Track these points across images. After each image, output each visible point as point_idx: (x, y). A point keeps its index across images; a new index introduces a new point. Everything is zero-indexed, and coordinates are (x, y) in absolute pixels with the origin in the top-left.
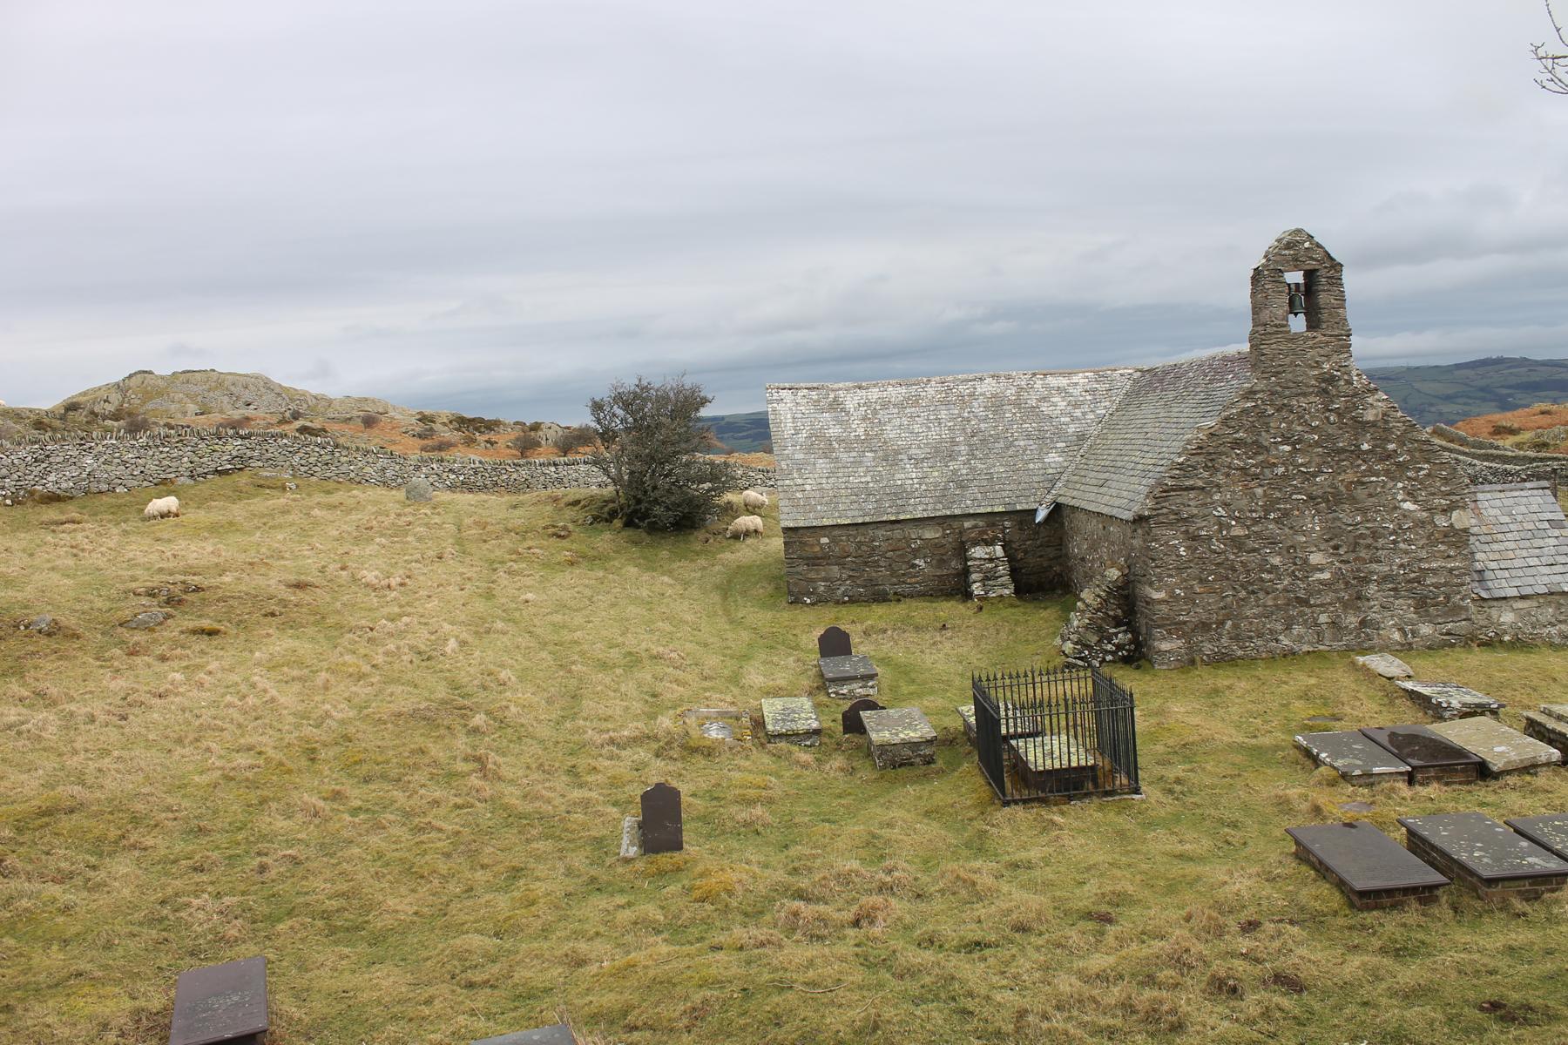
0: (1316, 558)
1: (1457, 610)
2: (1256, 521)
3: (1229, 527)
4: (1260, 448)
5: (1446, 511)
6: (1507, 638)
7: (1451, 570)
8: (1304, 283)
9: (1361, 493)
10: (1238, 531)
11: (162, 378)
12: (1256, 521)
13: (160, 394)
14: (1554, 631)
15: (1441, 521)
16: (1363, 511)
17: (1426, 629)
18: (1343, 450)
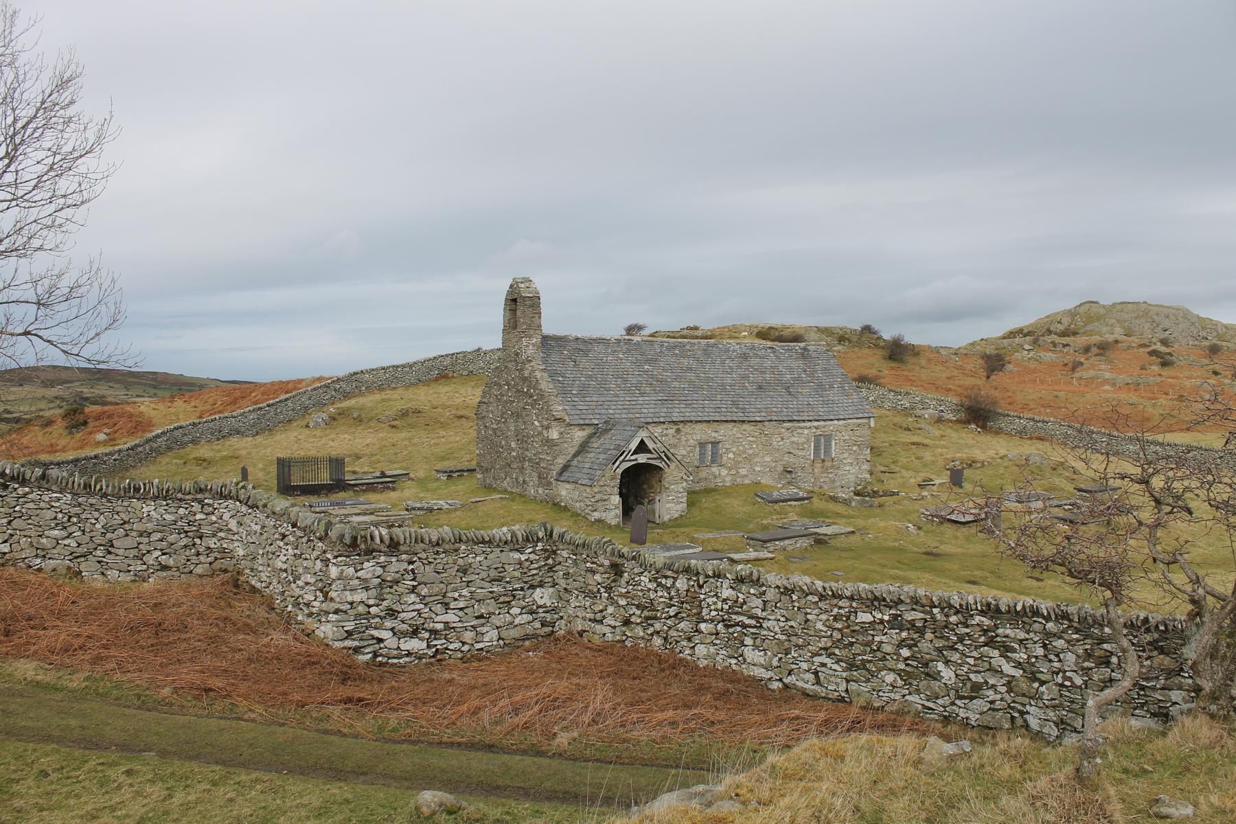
0: (513, 445)
2: (499, 422)
4: (501, 387)
8: (520, 305)
9: (524, 413)
11: (1104, 307)
12: (499, 422)
13: (1098, 319)
14: (578, 505)
15: (545, 432)
17: (540, 491)
18: (519, 391)
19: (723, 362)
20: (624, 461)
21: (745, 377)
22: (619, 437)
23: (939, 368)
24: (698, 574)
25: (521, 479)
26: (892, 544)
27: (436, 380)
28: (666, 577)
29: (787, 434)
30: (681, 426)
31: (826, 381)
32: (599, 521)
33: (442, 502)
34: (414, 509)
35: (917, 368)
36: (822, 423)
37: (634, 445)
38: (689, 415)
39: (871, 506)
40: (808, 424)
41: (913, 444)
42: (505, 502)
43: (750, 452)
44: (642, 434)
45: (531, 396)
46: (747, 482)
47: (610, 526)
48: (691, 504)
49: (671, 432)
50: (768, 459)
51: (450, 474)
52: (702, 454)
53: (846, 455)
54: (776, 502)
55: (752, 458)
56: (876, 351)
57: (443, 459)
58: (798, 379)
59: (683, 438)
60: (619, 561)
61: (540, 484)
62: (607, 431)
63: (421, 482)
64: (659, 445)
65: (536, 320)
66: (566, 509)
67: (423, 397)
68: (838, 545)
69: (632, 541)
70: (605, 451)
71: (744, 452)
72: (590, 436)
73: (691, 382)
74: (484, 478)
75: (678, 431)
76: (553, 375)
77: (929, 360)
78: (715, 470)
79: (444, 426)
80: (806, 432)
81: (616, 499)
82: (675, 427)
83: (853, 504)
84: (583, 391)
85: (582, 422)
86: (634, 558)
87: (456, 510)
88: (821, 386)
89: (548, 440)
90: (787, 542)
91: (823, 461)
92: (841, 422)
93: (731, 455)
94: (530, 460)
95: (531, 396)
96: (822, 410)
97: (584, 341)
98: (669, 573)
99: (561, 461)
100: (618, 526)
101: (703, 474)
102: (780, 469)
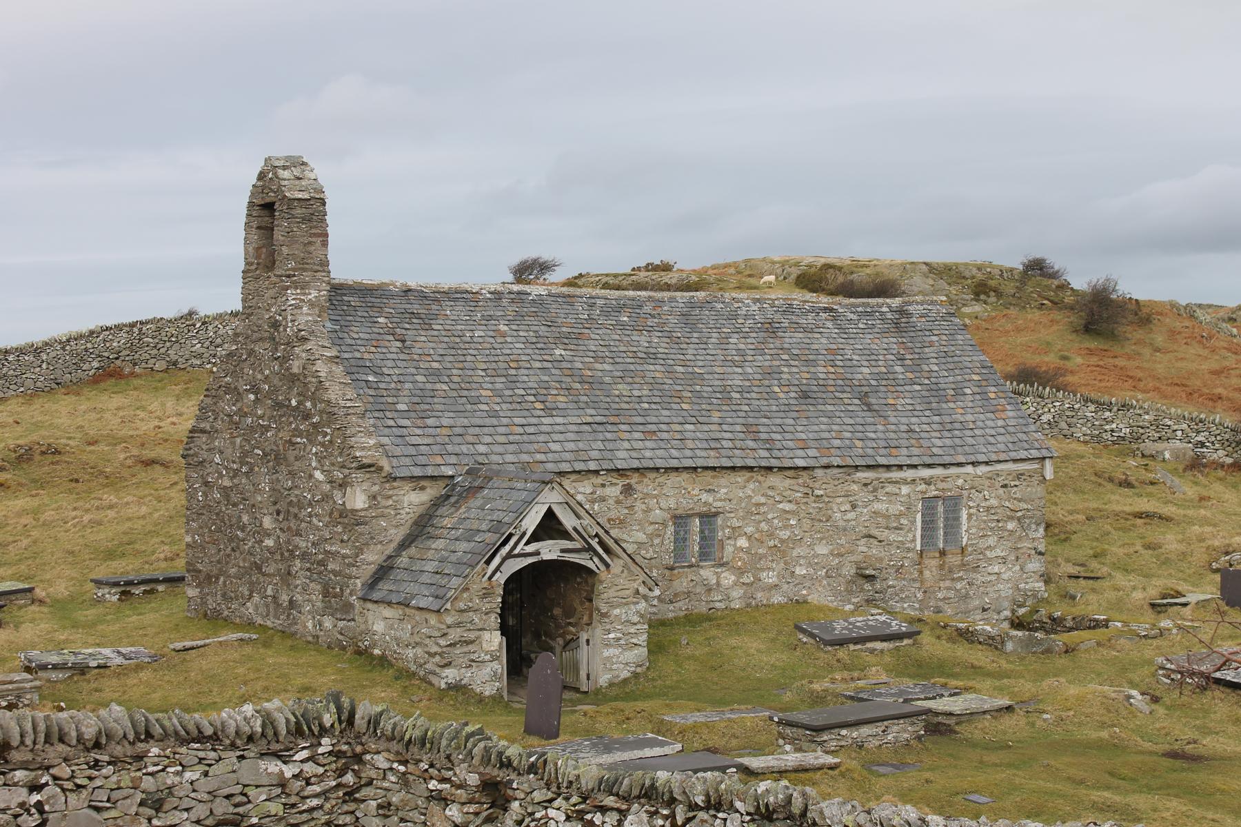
0: (268, 522)
1: (348, 607)
2: (236, 473)
3: (221, 476)
4: (239, 396)
5: (343, 485)
6: (377, 652)
7: (344, 557)
8: (282, 216)
10: (227, 483)
12: (236, 473)
14: (410, 653)
15: (337, 495)
16: (292, 474)
17: (328, 623)
18: (278, 405)
19: (724, 342)
20: (510, 555)
21: (770, 373)
22: (499, 504)
23: (1195, 349)
24: (672, 802)
25: (284, 598)
26: (1094, 735)
27: (96, 380)
28: (603, 810)
29: (863, 496)
30: (634, 480)
31: (948, 382)
32: (457, 688)
33: (107, 651)
34: (44, 667)
35: (1147, 352)
36: (939, 471)
37: (531, 522)
38: (651, 454)
39: (1048, 651)
40: (909, 474)
41: (1139, 515)
42: (248, 650)
43: (784, 534)
44: (551, 497)
45: (307, 416)
46: (777, 599)
47: (481, 699)
48: (656, 648)
49: (613, 491)
50: (822, 549)
51: (125, 589)
52: (681, 541)
53: (991, 541)
54: (841, 643)
55: (787, 549)
56: (1057, 315)
57: (110, 555)
58: (887, 377)
59: (639, 506)
60: (501, 775)
61: (328, 610)
62: (473, 491)
63: (62, 608)
64: (587, 521)
65: (316, 249)
66: (384, 662)
67: (64, 418)
68: (978, 735)
69: (529, 731)
70: (470, 535)
71: (771, 535)
72: (438, 503)
73: (654, 383)
74: (203, 597)
75: (628, 490)
76: (354, 369)
77: (1173, 334)
78: (707, 573)
79: (113, 481)
80: (905, 490)
81: (494, 640)
82: (621, 482)
83: (1009, 646)
84: (421, 407)
85: (417, 472)
86: (532, 769)
87: (139, 668)
88: (936, 392)
89: (344, 513)
90: (865, 730)
91: (943, 553)
92: (982, 470)
94: (305, 556)
95: (307, 416)
96: (938, 444)
97: (422, 295)
98: (610, 801)
99: (373, 557)
100: (497, 699)
101: (681, 584)
102: (849, 570)
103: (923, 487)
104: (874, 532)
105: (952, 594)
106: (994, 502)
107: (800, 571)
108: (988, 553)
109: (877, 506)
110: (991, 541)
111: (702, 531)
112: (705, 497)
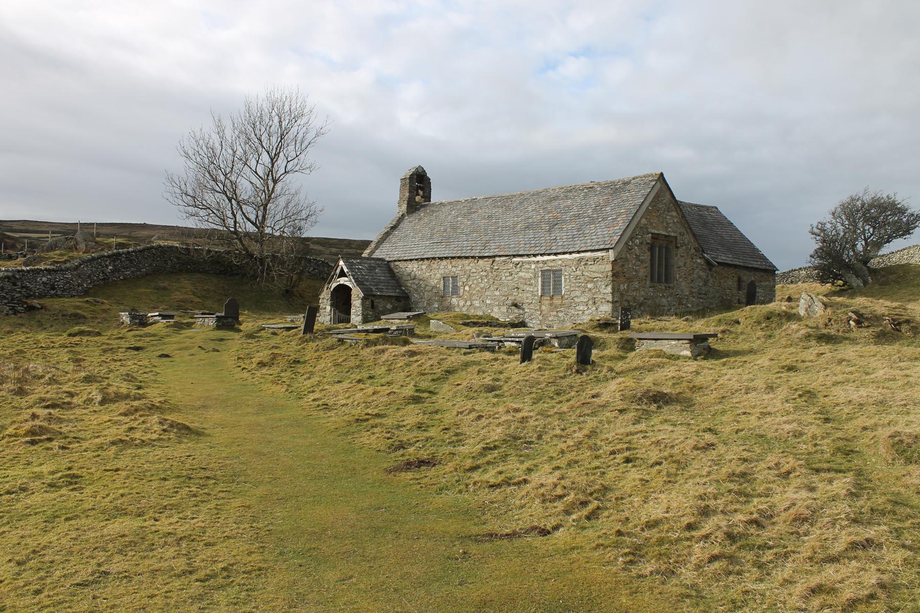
43: (482, 285)
49: (424, 267)
50: (497, 293)
80: (533, 266)
93: (467, 288)
102: (509, 302)
103: (541, 265)
104: (521, 286)
105: (556, 319)
106: (578, 273)
107: (488, 302)
108: (576, 300)
109: (521, 274)
110: (578, 293)
111: (453, 283)
112: (454, 269)
